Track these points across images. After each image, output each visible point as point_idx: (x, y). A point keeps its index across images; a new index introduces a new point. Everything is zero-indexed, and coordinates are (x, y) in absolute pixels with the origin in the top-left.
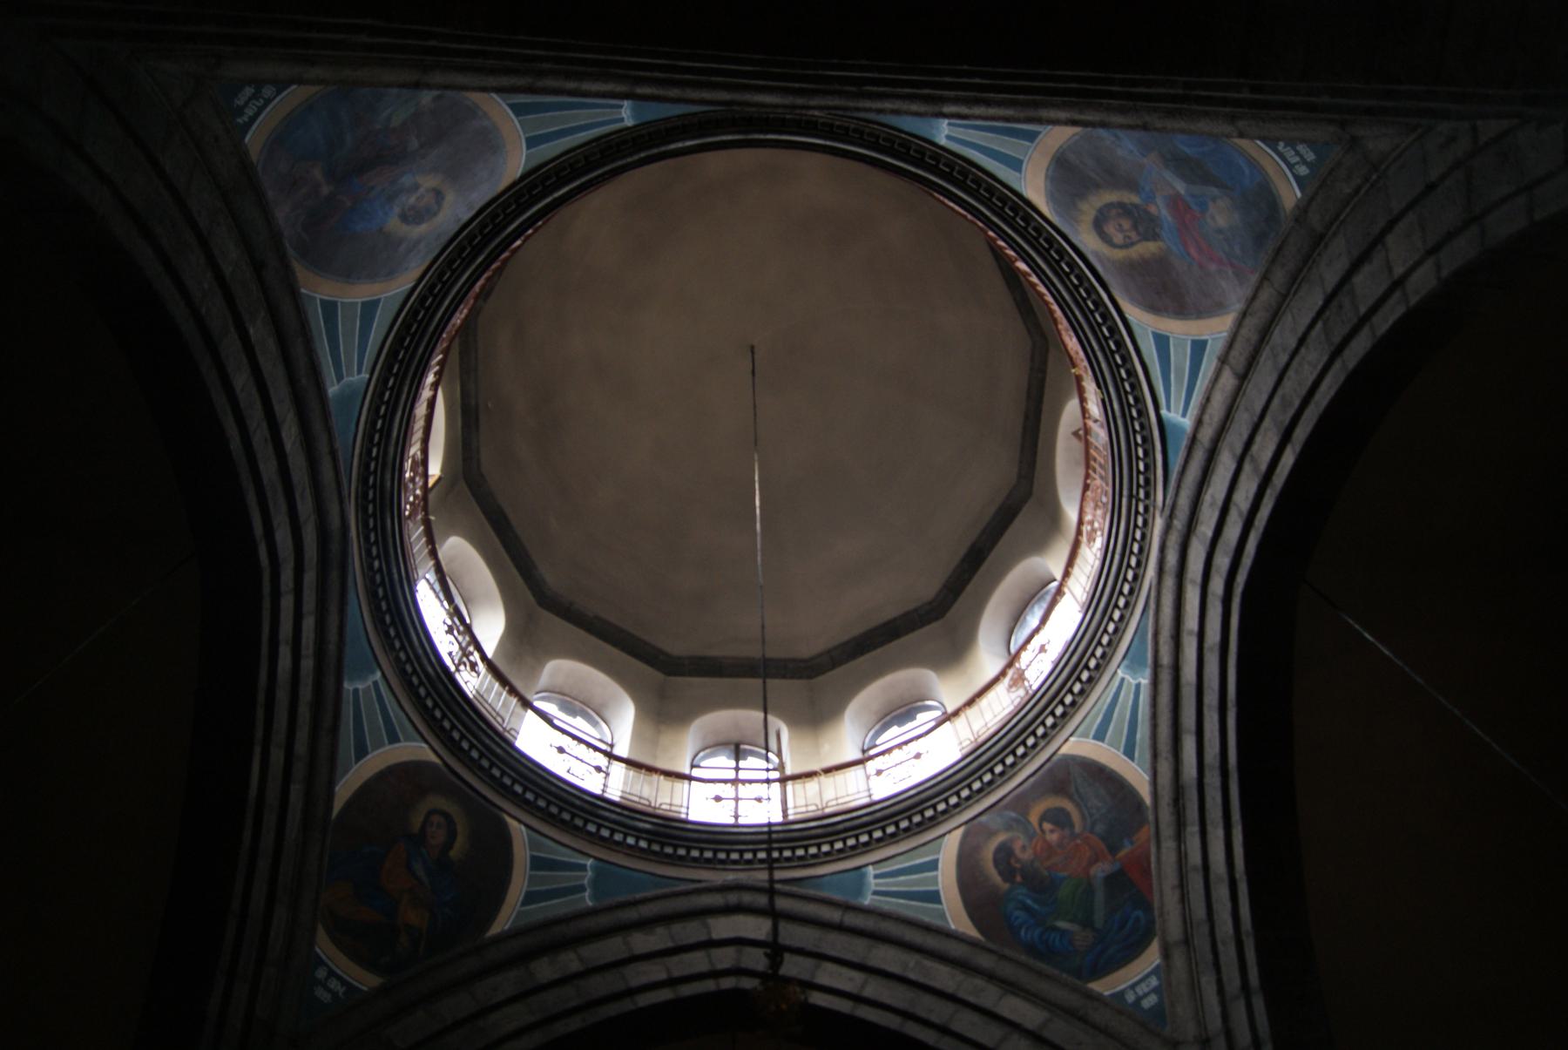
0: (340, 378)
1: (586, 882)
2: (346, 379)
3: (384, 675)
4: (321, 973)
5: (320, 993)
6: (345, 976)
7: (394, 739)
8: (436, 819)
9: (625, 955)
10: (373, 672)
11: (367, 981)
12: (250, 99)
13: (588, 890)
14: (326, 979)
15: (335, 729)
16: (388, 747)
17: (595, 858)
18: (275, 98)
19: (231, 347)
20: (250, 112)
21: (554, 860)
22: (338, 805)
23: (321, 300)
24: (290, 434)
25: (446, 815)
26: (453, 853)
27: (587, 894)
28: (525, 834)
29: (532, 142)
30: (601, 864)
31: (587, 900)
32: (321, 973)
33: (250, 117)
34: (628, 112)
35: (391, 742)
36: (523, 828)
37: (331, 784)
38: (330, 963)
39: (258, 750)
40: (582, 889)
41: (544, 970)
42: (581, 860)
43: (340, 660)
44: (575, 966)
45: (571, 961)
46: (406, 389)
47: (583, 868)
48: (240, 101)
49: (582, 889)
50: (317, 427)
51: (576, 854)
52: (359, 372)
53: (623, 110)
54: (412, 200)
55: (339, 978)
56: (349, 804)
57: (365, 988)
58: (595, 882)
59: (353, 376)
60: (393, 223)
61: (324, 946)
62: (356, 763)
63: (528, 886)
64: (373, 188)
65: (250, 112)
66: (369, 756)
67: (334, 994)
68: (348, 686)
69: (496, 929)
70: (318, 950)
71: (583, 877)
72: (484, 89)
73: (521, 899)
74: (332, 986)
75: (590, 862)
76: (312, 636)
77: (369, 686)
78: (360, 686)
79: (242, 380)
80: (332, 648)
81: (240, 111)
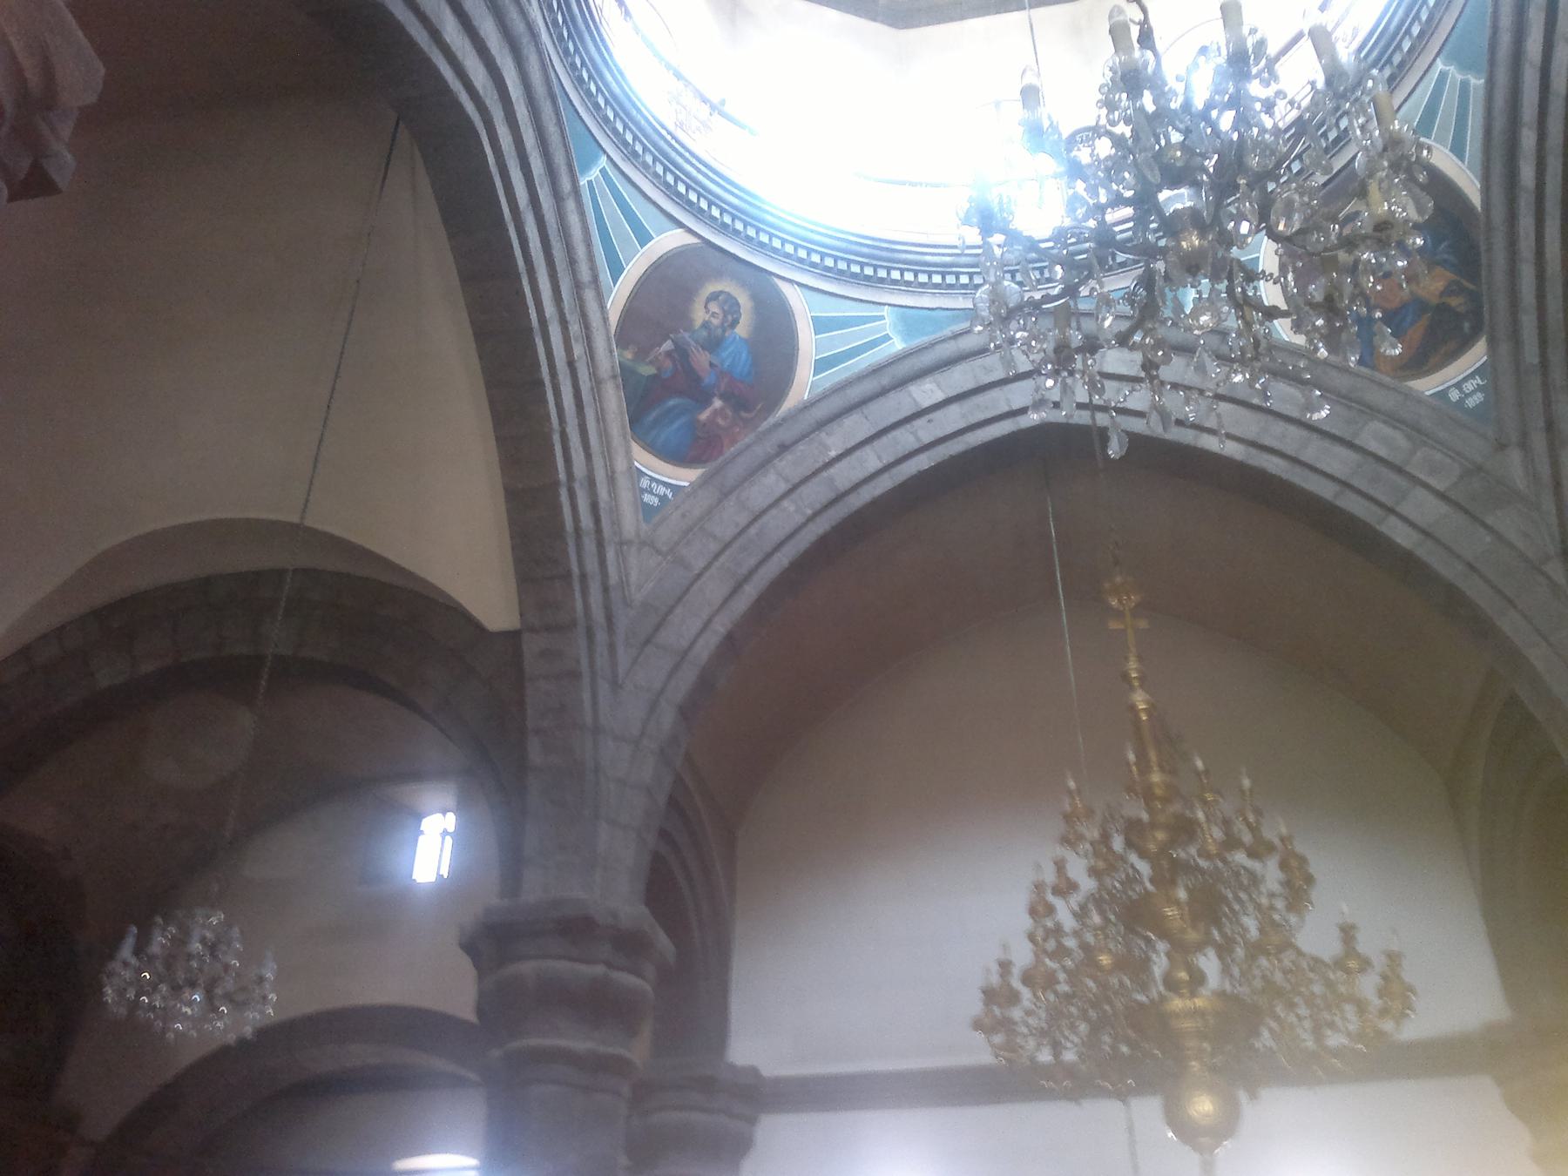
0: (887, 338)
1: (1459, 77)
2: (888, 332)
4: (1454, 395)
5: (1471, 402)
6: (1465, 374)
11: (1477, 354)
12: (654, 494)
14: (1461, 390)
17: (1438, 54)
18: (649, 476)
19: (845, 474)
20: (662, 490)
23: (814, 376)
24: (927, 392)
29: (644, 238)
30: (1444, 53)
31: (1477, 82)
32: (1454, 395)
33: (666, 488)
34: (592, 172)
38: (1446, 385)
40: (1465, 86)
41: (1527, 173)
42: (1434, 75)
45: (1528, 139)
46: (904, 256)
47: (1443, 75)
48: (654, 501)
49: (1465, 86)
50: (928, 359)
51: (1425, 80)
52: (882, 318)
53: (592, 178)
54: (715, 322)
55: (1465, 379)
58: (1464, 66)
59: (886, 323)
60: (742, 330)
61: (1427, 386)
63: (1445, 146)
64: (711, 365)
65: (662, 490)
67: (1479, 388)
69: (1476, 199)
70: (1427, 393)
71: (1453, 77)
72: (605, 320)
73: (1454, 158)
74: (1471, 388)
75: (1440, 65)
79: (871, 460)
81: (663, 498)
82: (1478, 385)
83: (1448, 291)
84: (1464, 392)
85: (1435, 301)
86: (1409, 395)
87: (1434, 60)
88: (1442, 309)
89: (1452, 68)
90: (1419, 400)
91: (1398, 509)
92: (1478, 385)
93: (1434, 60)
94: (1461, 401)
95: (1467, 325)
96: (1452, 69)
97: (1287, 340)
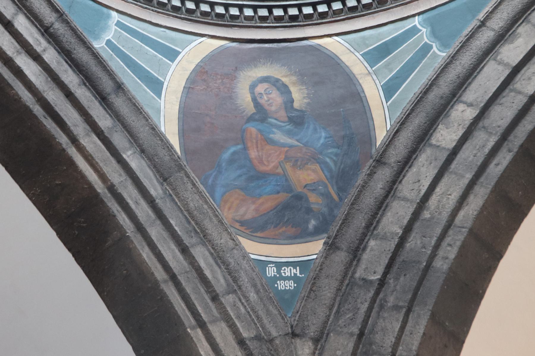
1: (426, 40)
3: (118, 11)
4: (271, 271)
5: (282, 285)
7: (172, 55)
8: (261, 88)
9: (507, 72)
10: (109, 17)
13: (434, 45)
14: (279, 271)
15: (119, 87)
16: (174, 65)
17: (419, 14)
21: (385, 44)
22: (175, 141)
25: (265, 80)
26: (296, 105)
27: (435, 48)
28: (342, 42)
32: (271, 271)
35: (173, 61)
36: (336, 38)
37: (154, 130)
39: (72, 152)
40: (427, 48)
43: (74, 31)
44: (470, 114)
47: (414, 30)
49: (427, 48)
55: (287, 264)
56: (183, 134)
57: (315, 257)
58: (434, 34)
62: (159, 96)
66: (165, 84)
67: (295, 278)
68: (98, 45)
70: (252, 256)
75: (416, 21)
76: (34, 30)
77: (116, 30)
78: (109, 36)
80: (59, 27)
82: (295, 274)
83: (312, 187)
84: (280, 274)
85: (300, 190)
86: (237, 245)
87: (414, 16)
88: (299, 197)
89: (424, 30)
90: (245, 256)
91: (211, 327)
92: (295, 274)
93: (414, 16)
94: (275, 279)
95: (313, 223)
96: (424, 30)
97: (164, 131)
